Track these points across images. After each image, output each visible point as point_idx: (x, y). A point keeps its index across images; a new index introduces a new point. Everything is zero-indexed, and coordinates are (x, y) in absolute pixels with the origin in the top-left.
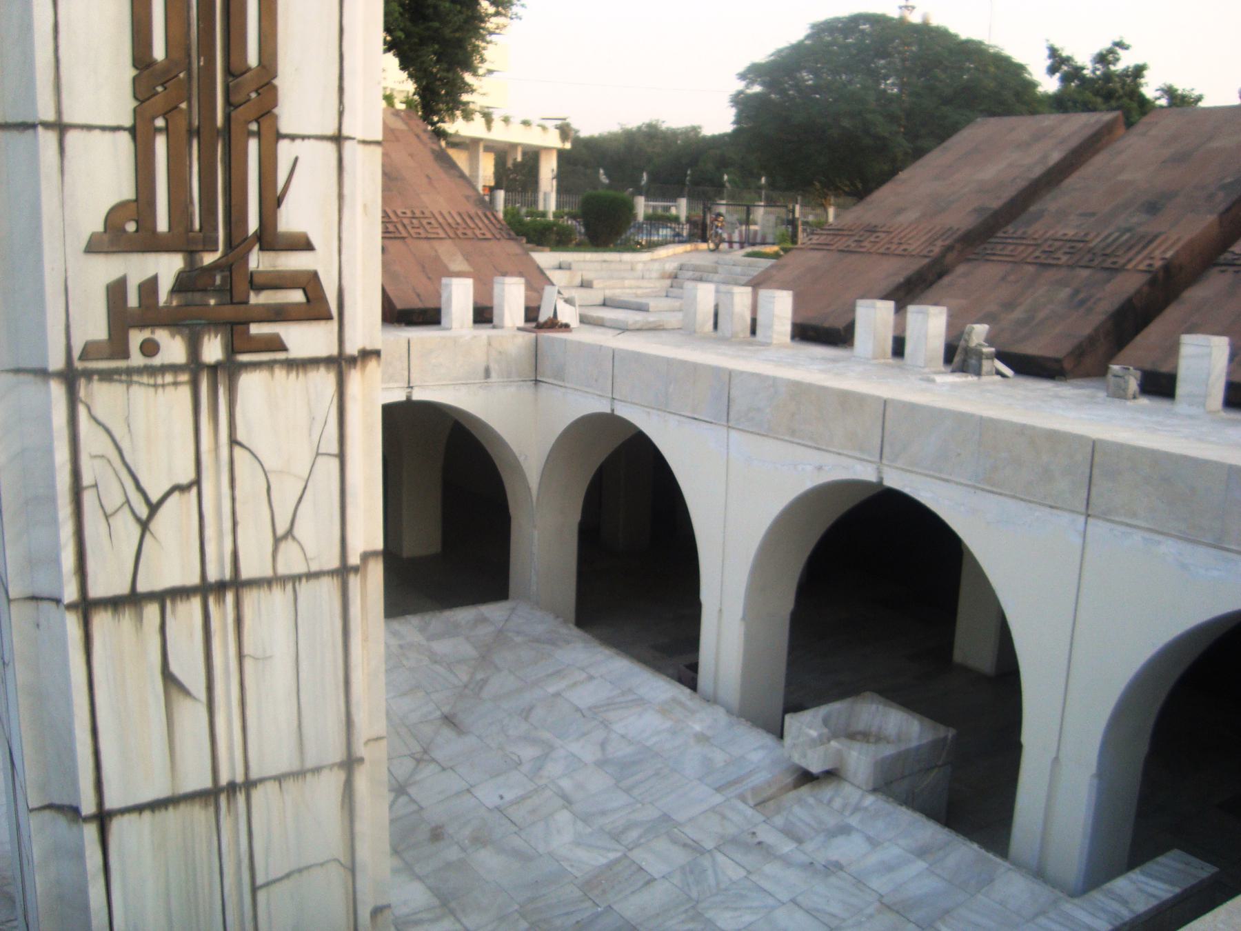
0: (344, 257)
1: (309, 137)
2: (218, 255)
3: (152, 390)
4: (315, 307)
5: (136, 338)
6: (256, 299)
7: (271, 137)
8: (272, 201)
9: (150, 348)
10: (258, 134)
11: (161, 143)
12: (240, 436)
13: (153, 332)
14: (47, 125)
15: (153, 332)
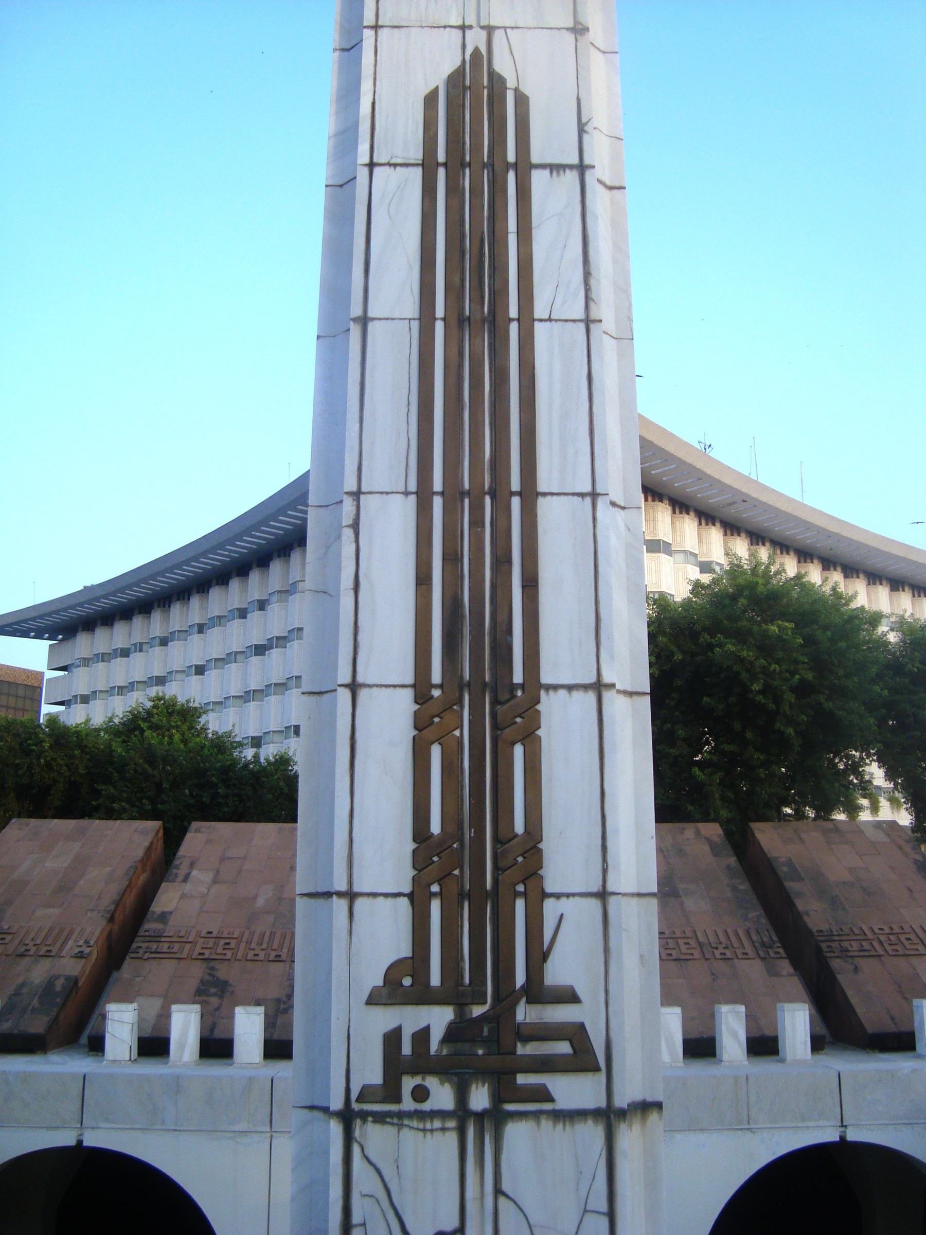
0: (610, 1009)
1: (574, 895)
2: (487, 1007)
3: (421, 1134)
4: (582, 1058)
5: (408, 1083)
6: (521, 1050)
7: (537, 897)
8: (538, 955)
9: (421, 1094)
10: (525, 894)
11: (435, 906)
12: (506, 1186)
13: (423, 1079)
14: (340, 894)
15: (423, 1079)
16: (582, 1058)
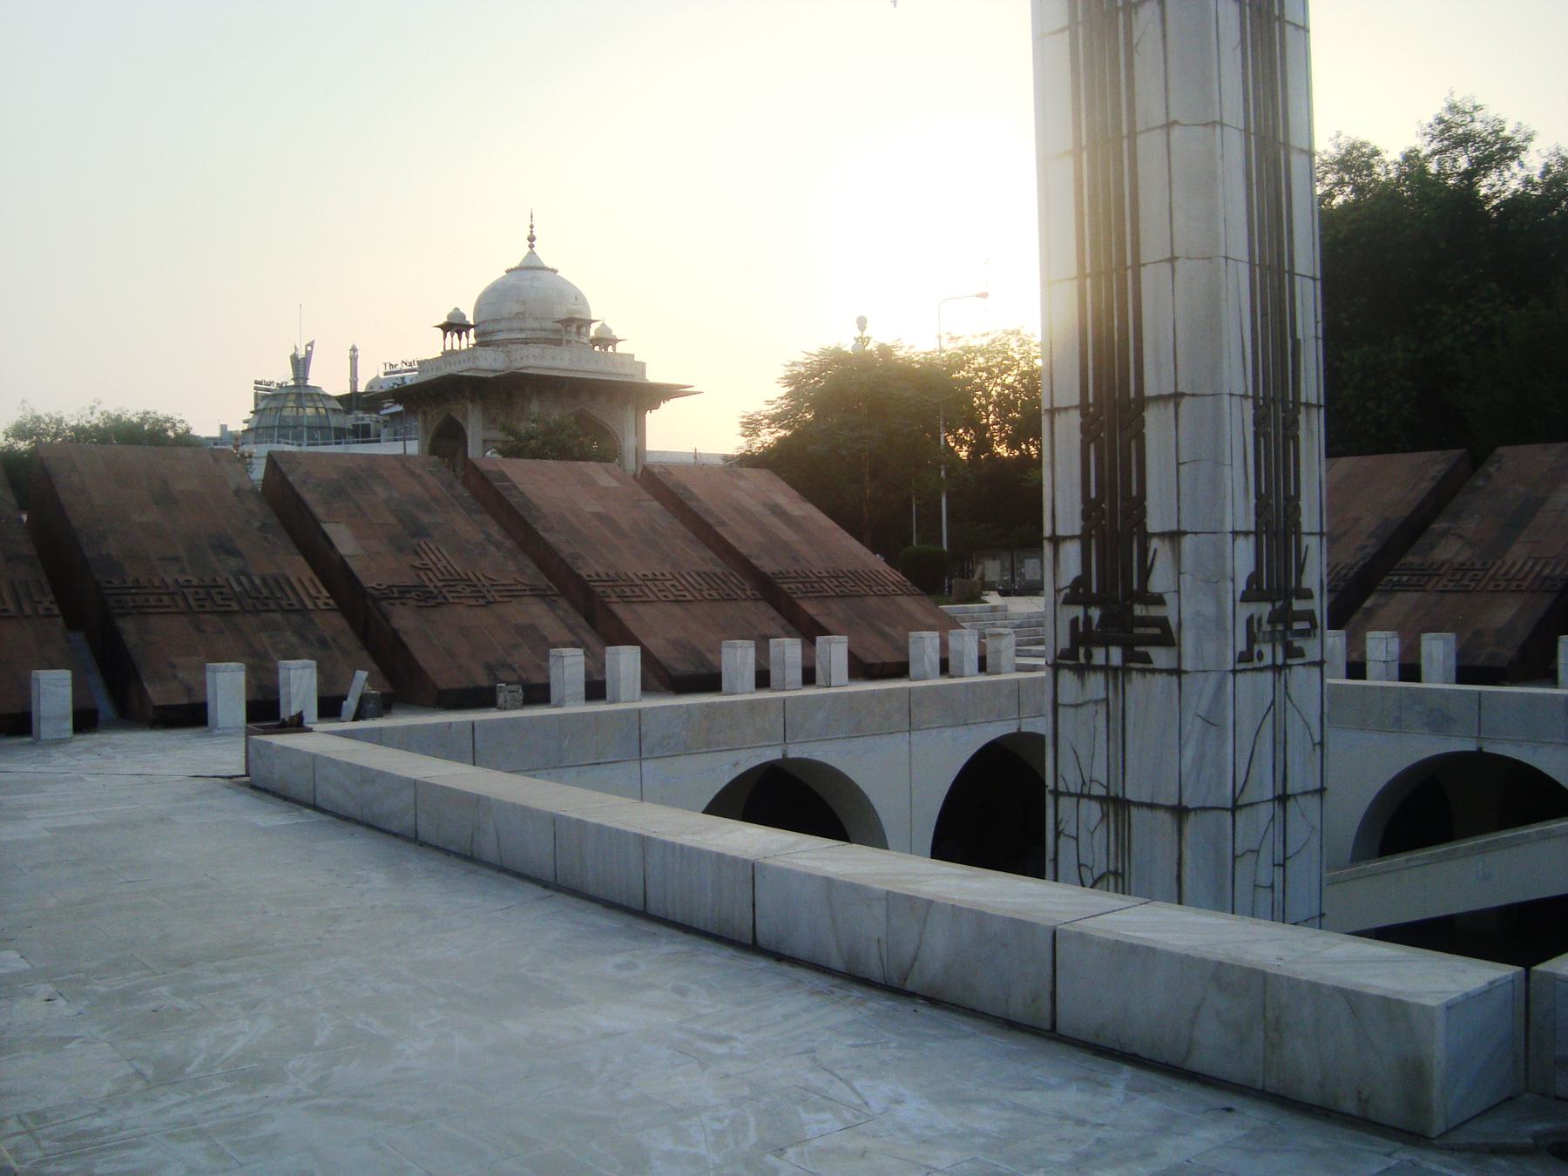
6: (1138, 631)
8: (1146, 572)
9: (1089, 656)
16: (1167, 638)
